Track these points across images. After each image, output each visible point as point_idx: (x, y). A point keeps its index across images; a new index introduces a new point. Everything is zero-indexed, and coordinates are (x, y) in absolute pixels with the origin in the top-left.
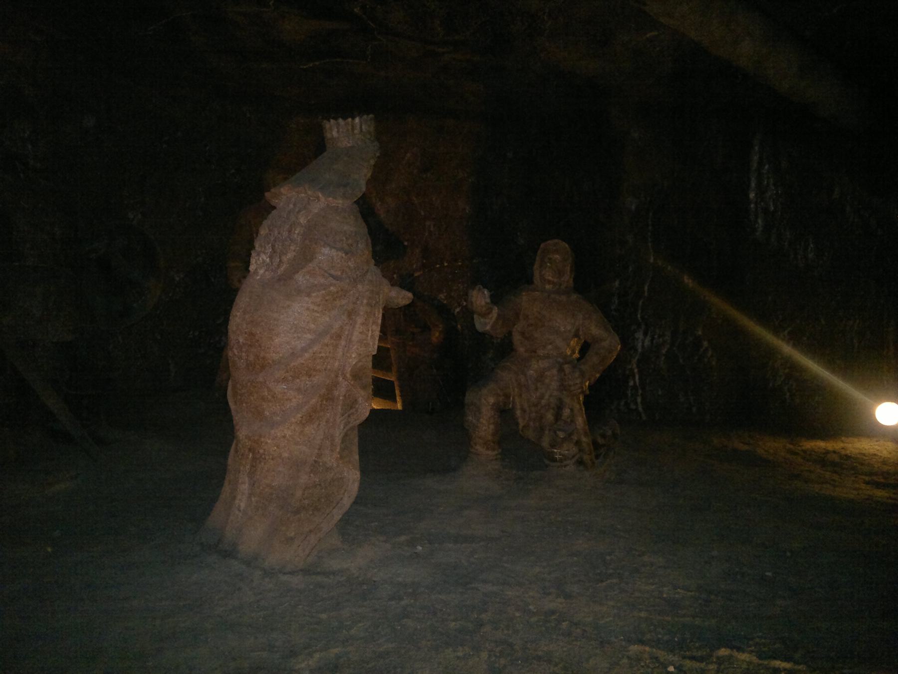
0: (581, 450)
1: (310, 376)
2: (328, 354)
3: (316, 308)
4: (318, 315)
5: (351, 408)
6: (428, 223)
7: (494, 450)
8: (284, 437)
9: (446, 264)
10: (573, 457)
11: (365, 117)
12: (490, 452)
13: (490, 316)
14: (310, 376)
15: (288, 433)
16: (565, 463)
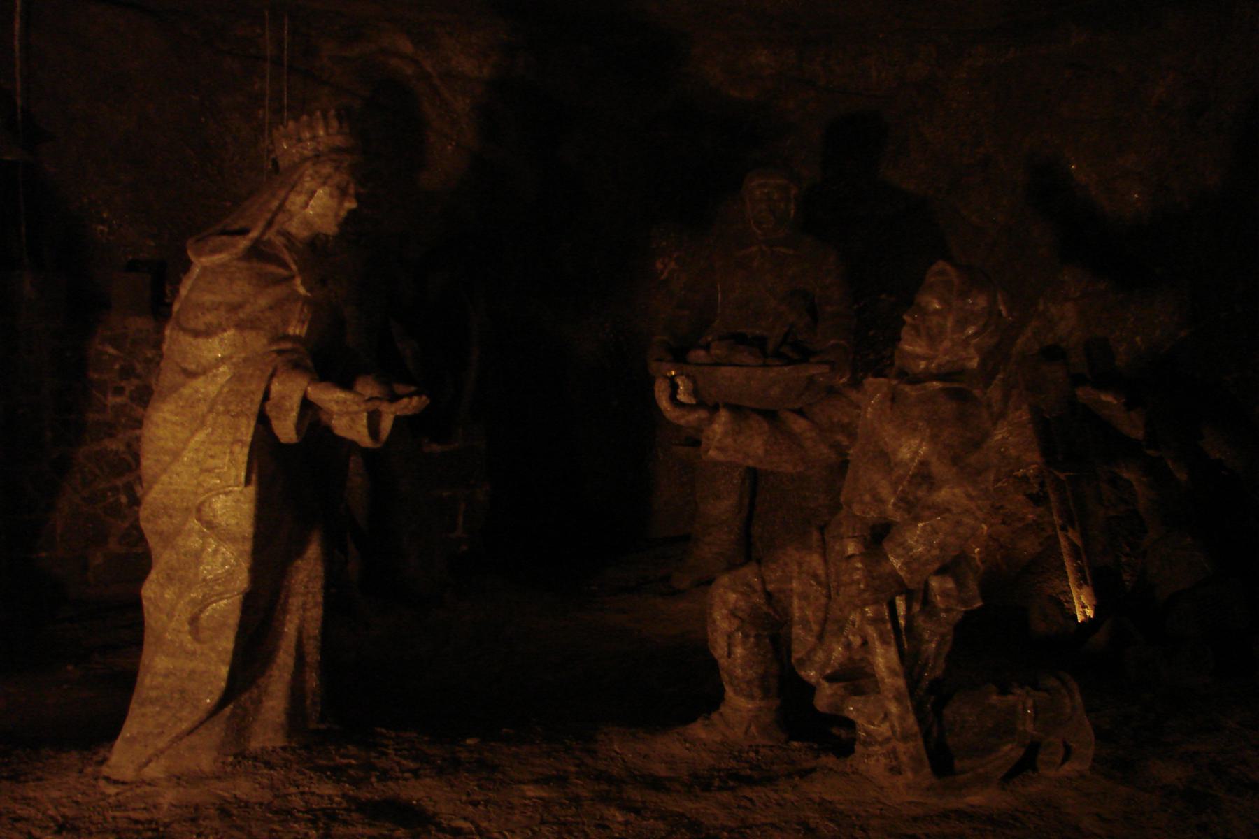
3: (175, 418)
4: (179, 428)
7: (751, 697)
14: (170, 517)
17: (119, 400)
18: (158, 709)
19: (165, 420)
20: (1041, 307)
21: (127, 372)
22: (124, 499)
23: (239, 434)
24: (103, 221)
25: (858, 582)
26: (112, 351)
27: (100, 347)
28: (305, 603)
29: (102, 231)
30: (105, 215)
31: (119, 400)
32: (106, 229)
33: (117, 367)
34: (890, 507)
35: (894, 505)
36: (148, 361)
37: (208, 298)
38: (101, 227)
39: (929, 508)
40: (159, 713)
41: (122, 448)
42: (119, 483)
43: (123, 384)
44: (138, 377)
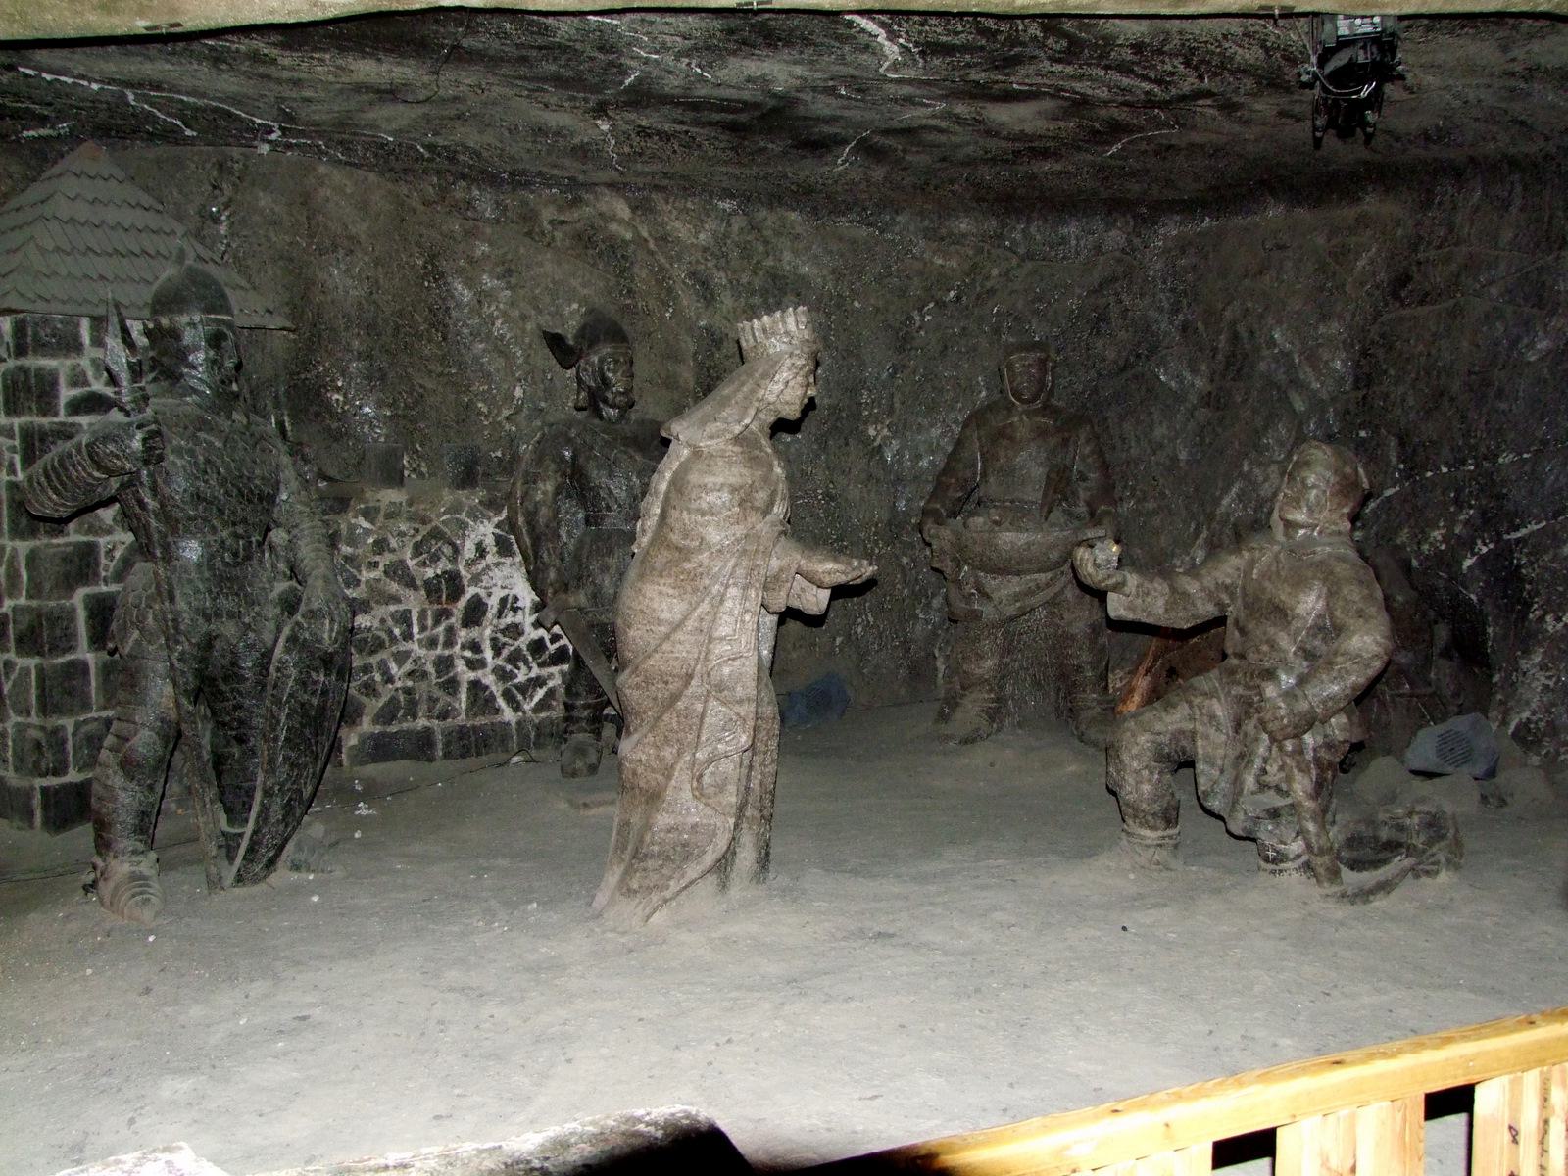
0: (1309, 846)
1: (667, 683)
2: (684, 654)
3: (671, 591)
5: (724, 729)
6: (1401, 390)
7: (1154, 828)
8: (640, 761)
9: (1445, 470)
10: (1299, 856)
11: (778, 314)
12: (1147, 833)
13: (1127, 590)
14: (667, 683)
15: (644, 757)
16: (1282, 866)
17: (373, 575)
18: (661, 863)
19: (660, 593)
20: (1246, 468)
21: (381, 546)
22: (378, 677)
23: (747, 604)
24: (338, 390)
25: (1282, 718)
26: (366, 525)
27: (353, 521)
28: (765, 760)
29: (338, 400)
30: (340, 384)
31: (373, 575)
32: (341, 398)
33: (371, 540)
34: (1291, 654)
35: (1295, 653)
36: (402, 534)
37: (709, 480)
38: (336, 396)
39: (1342, 654)
40: (662, 866)
41: (376, 624)
42: (374, 660)
43: (377, 558)
44: (393, 551)
